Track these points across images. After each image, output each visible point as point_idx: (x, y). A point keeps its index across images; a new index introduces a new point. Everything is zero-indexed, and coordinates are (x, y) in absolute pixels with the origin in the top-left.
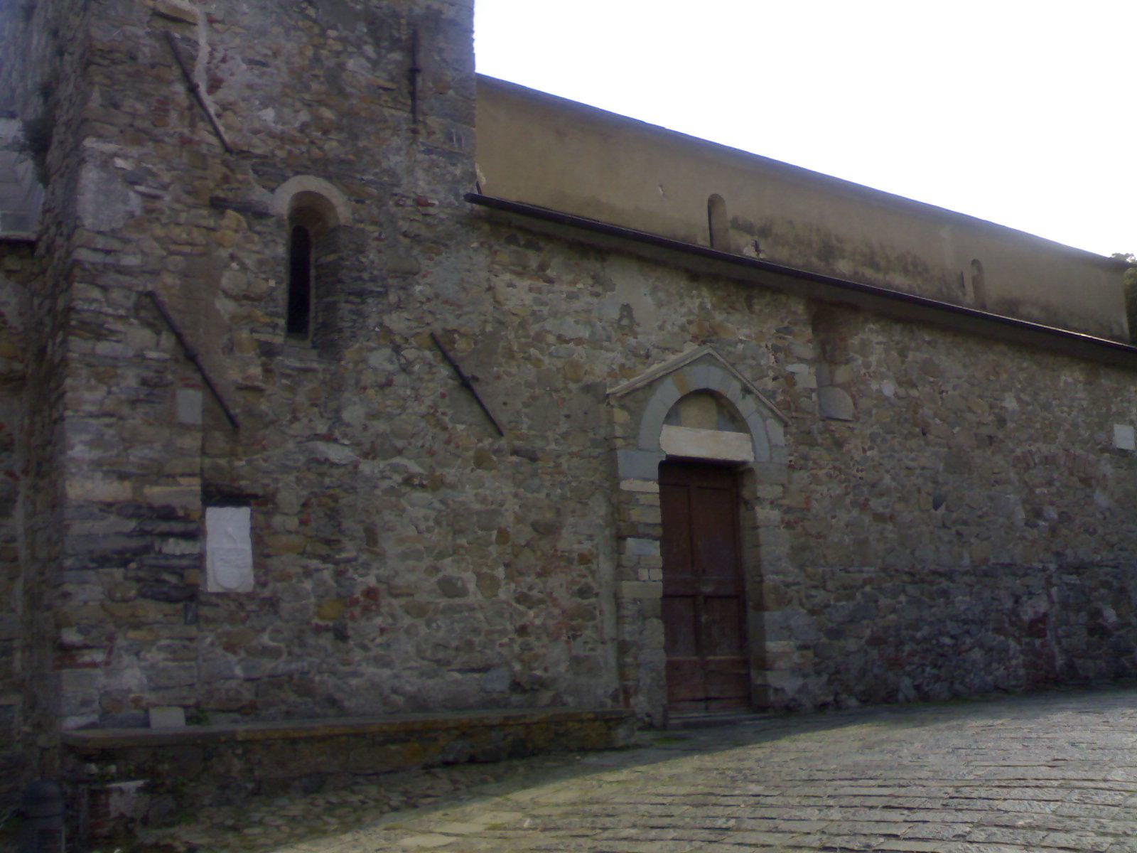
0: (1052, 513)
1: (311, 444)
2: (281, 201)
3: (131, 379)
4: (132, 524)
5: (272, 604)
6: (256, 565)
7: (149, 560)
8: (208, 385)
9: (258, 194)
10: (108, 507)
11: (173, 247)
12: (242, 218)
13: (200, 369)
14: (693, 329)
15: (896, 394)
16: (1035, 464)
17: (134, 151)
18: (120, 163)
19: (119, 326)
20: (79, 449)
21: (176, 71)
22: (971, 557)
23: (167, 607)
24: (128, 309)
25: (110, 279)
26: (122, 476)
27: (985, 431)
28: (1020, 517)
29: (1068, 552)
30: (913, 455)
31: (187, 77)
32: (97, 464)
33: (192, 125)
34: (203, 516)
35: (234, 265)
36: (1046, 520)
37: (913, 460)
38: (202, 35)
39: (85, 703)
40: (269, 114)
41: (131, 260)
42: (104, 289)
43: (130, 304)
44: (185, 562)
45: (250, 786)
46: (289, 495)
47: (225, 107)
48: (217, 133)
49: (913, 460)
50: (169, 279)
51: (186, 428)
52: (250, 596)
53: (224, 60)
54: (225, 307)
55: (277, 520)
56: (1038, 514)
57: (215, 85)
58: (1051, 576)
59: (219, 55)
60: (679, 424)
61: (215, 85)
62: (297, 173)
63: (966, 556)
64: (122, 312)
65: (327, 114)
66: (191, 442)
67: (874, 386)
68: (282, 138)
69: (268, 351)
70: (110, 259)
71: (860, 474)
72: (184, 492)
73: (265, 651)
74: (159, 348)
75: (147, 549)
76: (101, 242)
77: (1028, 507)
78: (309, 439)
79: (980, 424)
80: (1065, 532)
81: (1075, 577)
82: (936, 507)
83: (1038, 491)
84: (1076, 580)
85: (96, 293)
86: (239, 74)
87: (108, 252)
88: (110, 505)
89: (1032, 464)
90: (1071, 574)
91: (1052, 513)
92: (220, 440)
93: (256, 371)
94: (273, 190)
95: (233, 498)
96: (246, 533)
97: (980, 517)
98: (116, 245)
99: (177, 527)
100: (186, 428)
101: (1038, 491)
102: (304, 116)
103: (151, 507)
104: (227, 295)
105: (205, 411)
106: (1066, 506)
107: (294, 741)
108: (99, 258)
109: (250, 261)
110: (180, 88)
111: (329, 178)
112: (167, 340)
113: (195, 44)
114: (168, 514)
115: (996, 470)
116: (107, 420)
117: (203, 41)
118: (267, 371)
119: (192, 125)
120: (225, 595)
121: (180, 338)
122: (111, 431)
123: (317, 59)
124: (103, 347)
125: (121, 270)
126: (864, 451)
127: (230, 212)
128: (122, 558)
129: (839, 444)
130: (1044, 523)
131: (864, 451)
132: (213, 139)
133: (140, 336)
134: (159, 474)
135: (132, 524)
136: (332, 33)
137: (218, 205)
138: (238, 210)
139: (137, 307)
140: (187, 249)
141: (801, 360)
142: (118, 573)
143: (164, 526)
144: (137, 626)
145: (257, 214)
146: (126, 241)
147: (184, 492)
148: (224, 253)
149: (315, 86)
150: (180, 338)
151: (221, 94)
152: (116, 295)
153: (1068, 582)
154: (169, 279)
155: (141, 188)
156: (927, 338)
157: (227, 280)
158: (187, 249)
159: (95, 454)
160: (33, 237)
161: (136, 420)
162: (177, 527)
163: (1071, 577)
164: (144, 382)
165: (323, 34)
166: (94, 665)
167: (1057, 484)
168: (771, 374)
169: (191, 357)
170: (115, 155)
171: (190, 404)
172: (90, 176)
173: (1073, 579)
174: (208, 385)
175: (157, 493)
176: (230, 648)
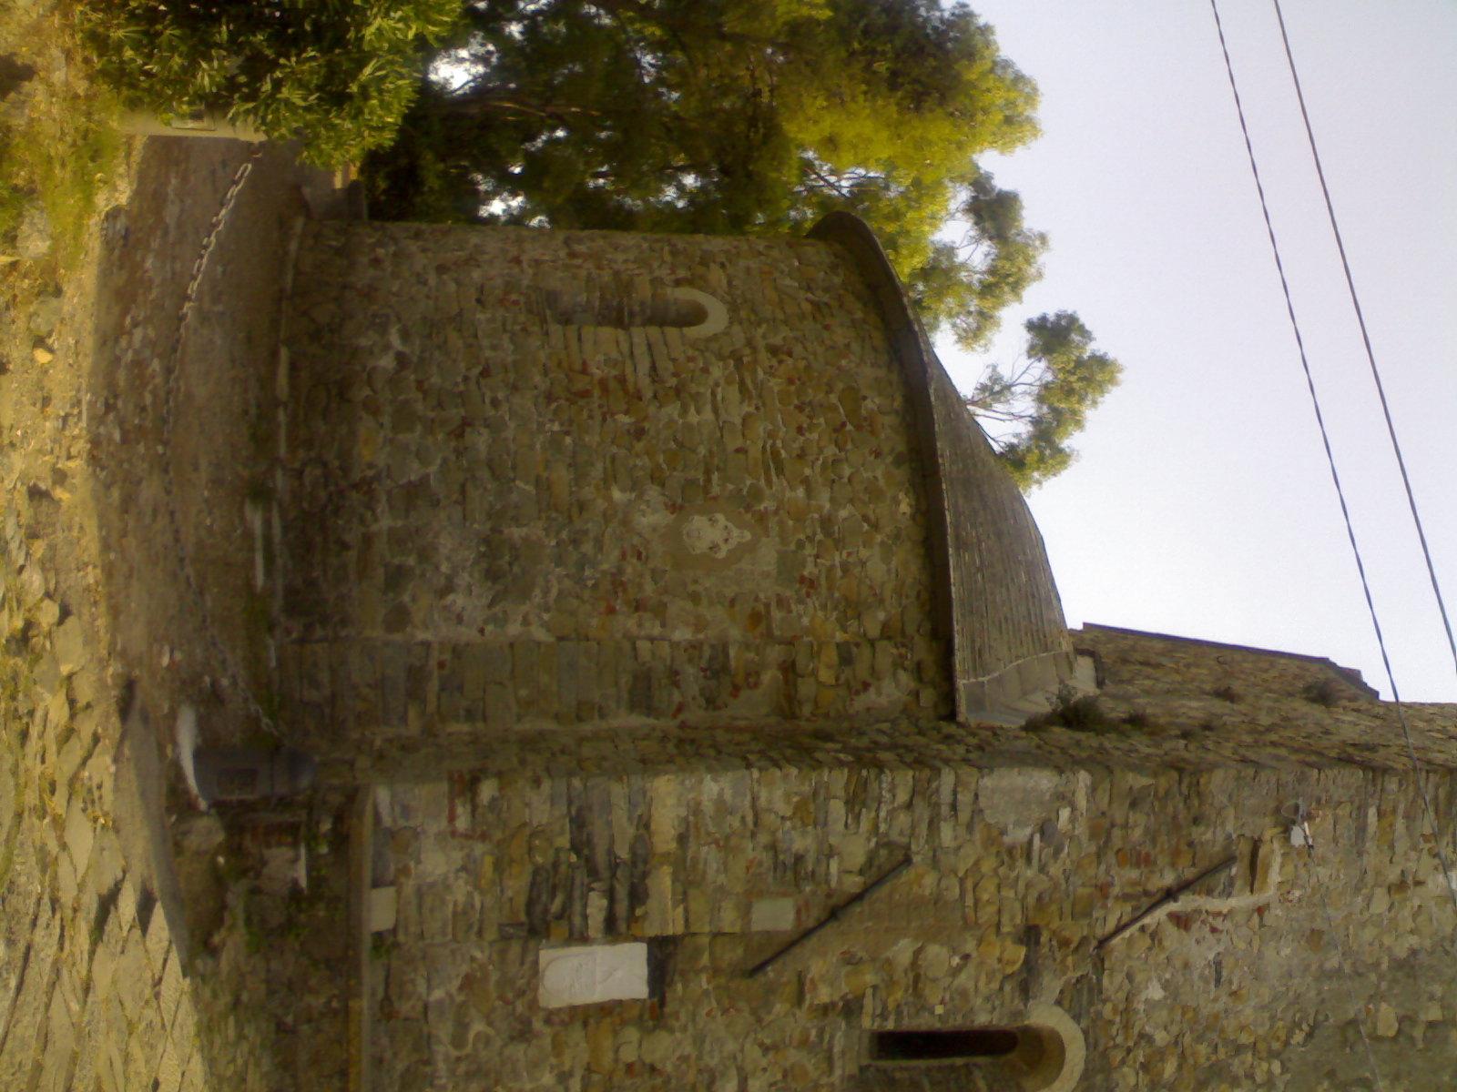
1: (733, 1072)
2: (1045, 1015)
3: (802, 842)
4: (623, 853)
5: (523, 1033)
6: (573, 1009)
7: (581, 877)
8: (803, 935)
9: (1051, 984)
10: (645, 824)
11: (969, 884)
12: (1017, 966)
13: (821, 924)
17: (1081, 830)
18: (1065, 814)
19: (865, 824)
20: (712, 788)
21: (1189, 873)
23: (521, 900)
24: (886, 835)
25: (923, 812)
26: (682, 839)
31: (1184, 887)
32: (696, 810)
33: (1126, 897)
34: (636, 939)
35: (956, 960)
38: (1241, 901)
39: (406, 811)
40: (1155, 992)
41: (947, 834)
42: (909, 806)
43: (894, 836)
44: (577, 920)
45: (289, 1019)
46: (664, 1048)
47: (1155, 936)
48: (1120, 929)
50: (930, 880)
51: (746, 911)
52: (533, 1005)
53: (1214, 930)
54: (902, 951)
55: (632, 1034)
57: (1181, 921)
59: (1218, 923)
61: (1181, 921)
62: (1085, 1032)
64: (883, 827)
65: (1170, 1068)
66: (729, 919)
68: (1127, 1011)
69: (851, 1008)
70: (945, 810)
72: (665, 915)
73: (462, 1025)
74: (843, 874)
75: (593, 873)
76: (965, 798)
78: (740, 1069)
85: (903, 797)
86: (1200, 950)
87: (954, 807)
88: (647, 826)
92: (732, 955)
93: (824, 995)
94: (1059, 1003)
95: (660, 974)
96: (617, 996)
98: (964, 816)
99: (622, 908)
100: (746, 911)
102: (1161, 1038)
103: (645, 875)
104: (917, 953)
105: (768, 934)
107: (344, 1074)
108: (946, 796)
109: (963, 979)
110: (1169, 879)
111: (1086, 1075)
112: (853, 883)
113: (1227, 893)
114: (638, 895)
116: (750, 819)
117: (1233, 902)
118: (825, 1009)
119: (1126, 897)
120: (535, 972)
121: (858, 897)
122: (737, 824)
123: (1239, 1049)
124: (837, 808)
125: (933, 825)
127: (1022, 951)
128: (580, 845)
132: (1111, 924)
133: (856, 850)
134: (687, 879)
135: (623, 853)
136: (1276, 1067)
137: (1030, 935)
138: (1027, 961)
139: (889, 845)
140: (969, 901)
142: (564, 841)
143: (622, 892)
144: (498, 866)
145: (1026, 983)
146: (970, 827)
147: (665, 915)
148: (970, 946)
149: (1203, 1049)
150: (858, 897)
151: (1171, 931)
152: (903, 819)
154: (930, 880)
155: (1037, 838)
157: (935, 951)
158: (969, 901)
159: (708, 807)
160: (961, 718)
161: (752, 850)
162: (622, 908)
164: (799, 858)
165: (1273, 1055)
166: (452, 818)
169: (834, 914)
170: (1074, 809)
171: (777, 915)
172: (1044, 781)
174: (803, 935)
175: (662, 882)
176: (468, 983)
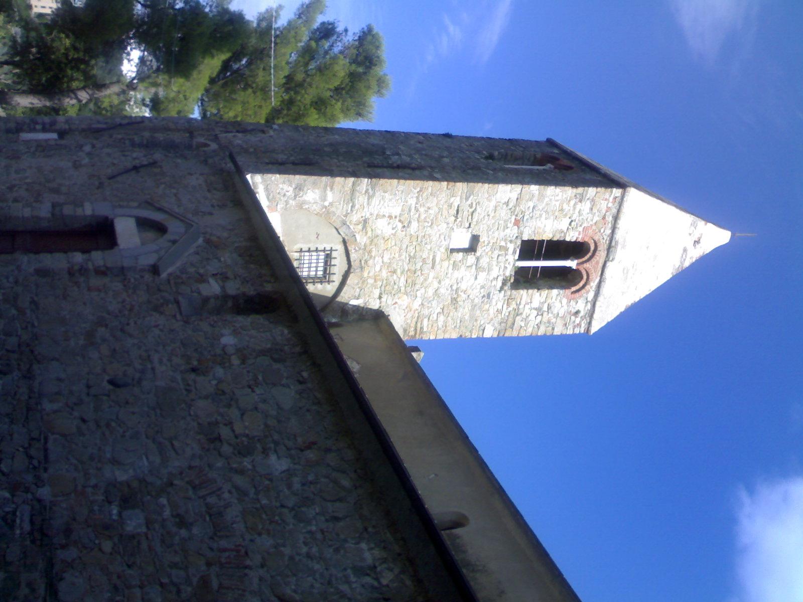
0: (134, 523)
14: (214, 239)
15: (225, 346)
16: (203, 497)
22: (55, 412)
27: (225, 432)
28: (117, 473)
29: (72, 553)
30: (165, 360)
36: (120, 514)
37: (161, 361)
49: (161, 361)
56: (127, 502)
58: (27, 490)
60: (139, 231)
63: (55, 406)
67: (226, 331)
71: (132, 324)
77: (135, 484)
79: (230, 424)
80: (107, 546)
81: (27, 527)
82: (111, 382)
83: (163, 500)
84: (22, 528)
89: (202, 492)
90: (32, 522)
91: (134, 523)
97: (108, 425)
101: (163, 500)
106: (150, 548)
115: (176, 443)
126: (156, 326)
129: (157, 309)
130: (115, 512)
131: (156, 326)
141: (223, 288)
153: (18, 513)
156: (305, 374)
163: (27, 518)
167: (184, 532)
168: (202, 271)
173: (23, 524)
